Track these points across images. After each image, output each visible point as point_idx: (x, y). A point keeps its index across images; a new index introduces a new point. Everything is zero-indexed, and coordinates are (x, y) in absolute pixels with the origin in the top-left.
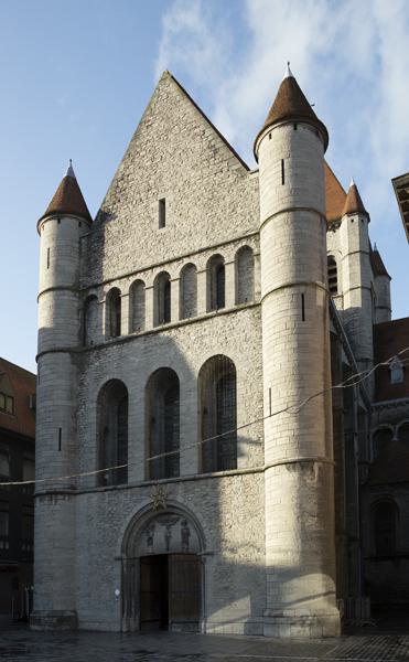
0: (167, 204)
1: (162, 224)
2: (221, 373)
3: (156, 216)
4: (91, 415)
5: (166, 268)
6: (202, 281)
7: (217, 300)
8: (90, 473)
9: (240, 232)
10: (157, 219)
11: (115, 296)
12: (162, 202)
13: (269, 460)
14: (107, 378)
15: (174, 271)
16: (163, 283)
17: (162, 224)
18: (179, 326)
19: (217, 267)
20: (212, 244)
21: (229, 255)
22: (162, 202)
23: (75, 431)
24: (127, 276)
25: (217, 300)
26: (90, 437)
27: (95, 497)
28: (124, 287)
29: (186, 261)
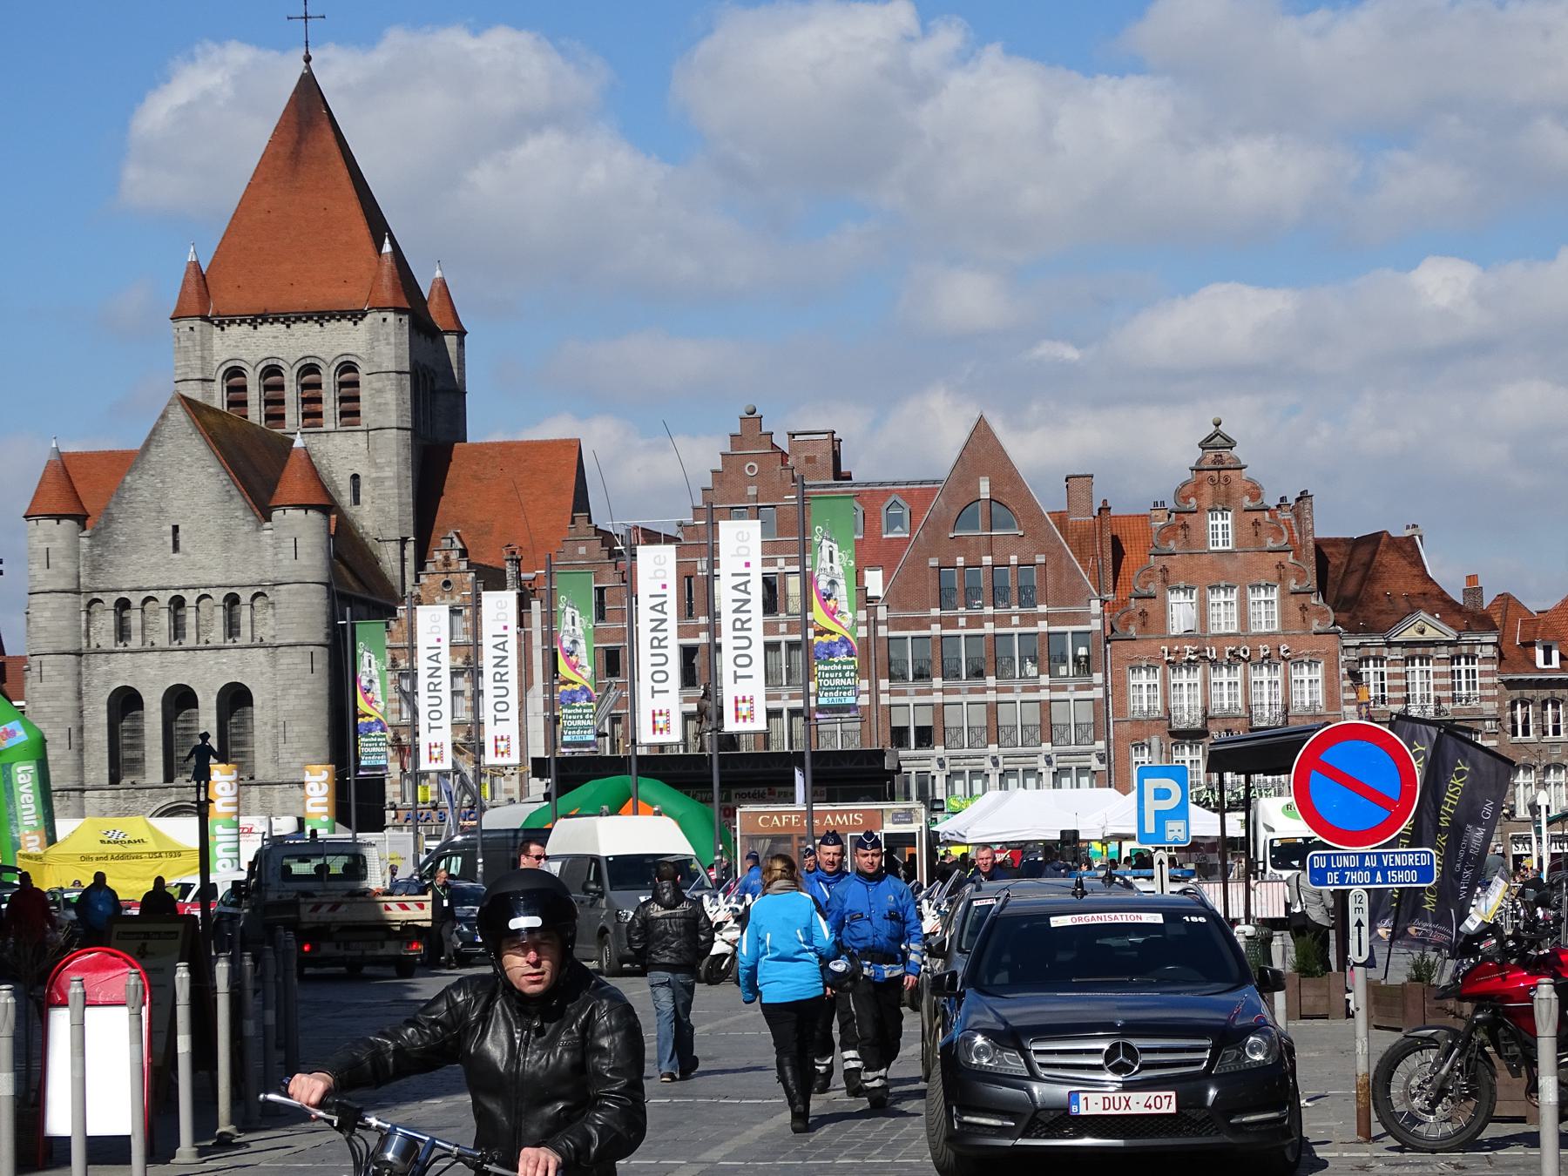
0: (181, 533)
1: (176, 548)
2: (235, 699)
3: (169, 539)
4: (98, 716)
5: (181, 592)
6: (220, 612)
7: (232, 629)
8: (98, 768)
9: (256, 578)
10: (171, 543)
11: (123, 605)
12: (176, 529)
13: (285, 778)
14: (119, 684)
15: (190, 597)
16: (178, 603)
17: (176, 548)
18: (194, 649)
19: (232, 600)
20: (228, 582)
21: (245, 596)
22: (176, 529)
23: (81, 729)
24: (139, 590)
25: (232, 629)
26: (98, 736)
27: (108, 794)
28: (136, 599)
29: (203, 592)
